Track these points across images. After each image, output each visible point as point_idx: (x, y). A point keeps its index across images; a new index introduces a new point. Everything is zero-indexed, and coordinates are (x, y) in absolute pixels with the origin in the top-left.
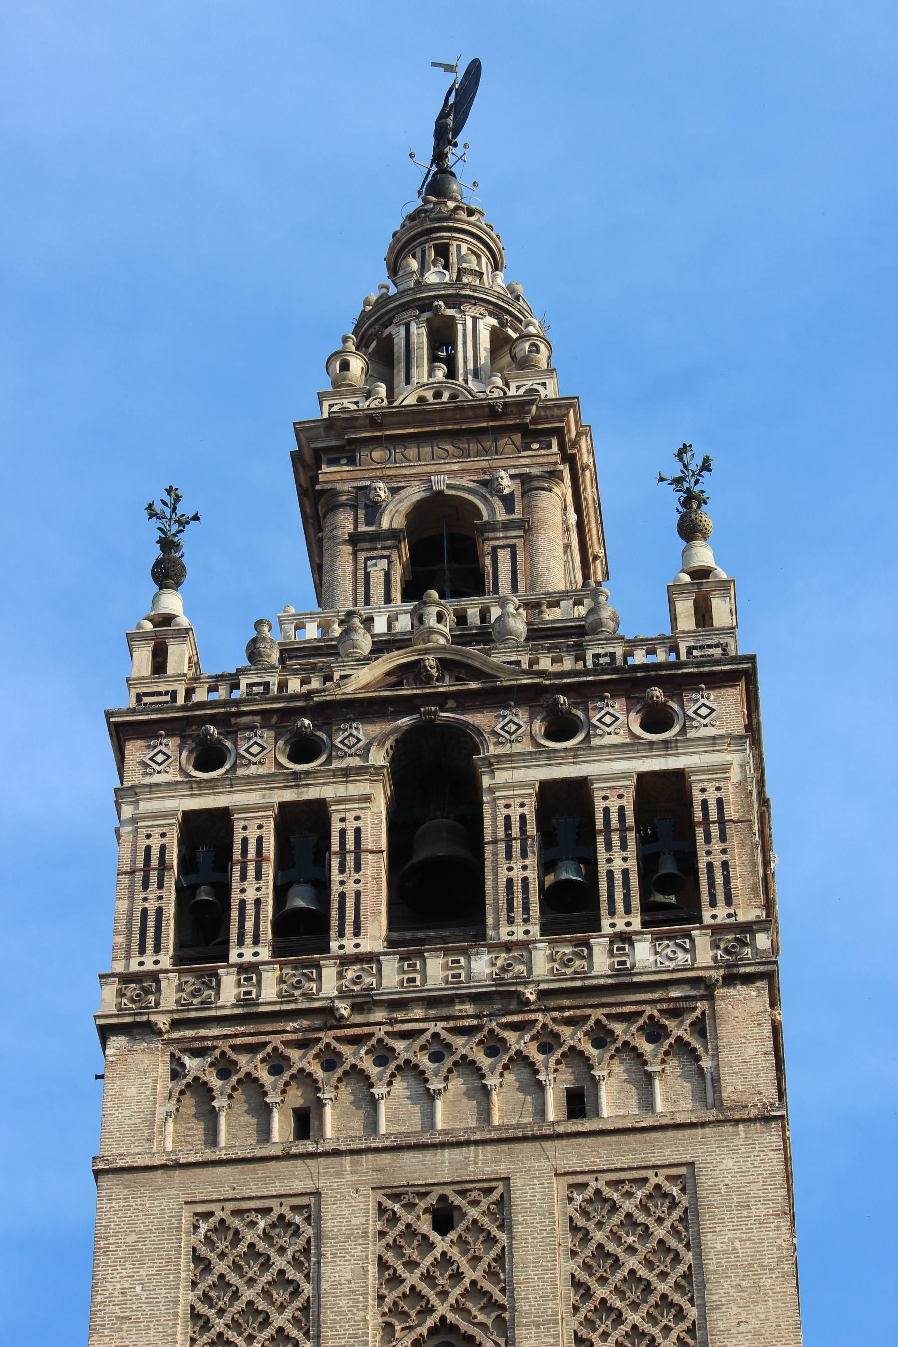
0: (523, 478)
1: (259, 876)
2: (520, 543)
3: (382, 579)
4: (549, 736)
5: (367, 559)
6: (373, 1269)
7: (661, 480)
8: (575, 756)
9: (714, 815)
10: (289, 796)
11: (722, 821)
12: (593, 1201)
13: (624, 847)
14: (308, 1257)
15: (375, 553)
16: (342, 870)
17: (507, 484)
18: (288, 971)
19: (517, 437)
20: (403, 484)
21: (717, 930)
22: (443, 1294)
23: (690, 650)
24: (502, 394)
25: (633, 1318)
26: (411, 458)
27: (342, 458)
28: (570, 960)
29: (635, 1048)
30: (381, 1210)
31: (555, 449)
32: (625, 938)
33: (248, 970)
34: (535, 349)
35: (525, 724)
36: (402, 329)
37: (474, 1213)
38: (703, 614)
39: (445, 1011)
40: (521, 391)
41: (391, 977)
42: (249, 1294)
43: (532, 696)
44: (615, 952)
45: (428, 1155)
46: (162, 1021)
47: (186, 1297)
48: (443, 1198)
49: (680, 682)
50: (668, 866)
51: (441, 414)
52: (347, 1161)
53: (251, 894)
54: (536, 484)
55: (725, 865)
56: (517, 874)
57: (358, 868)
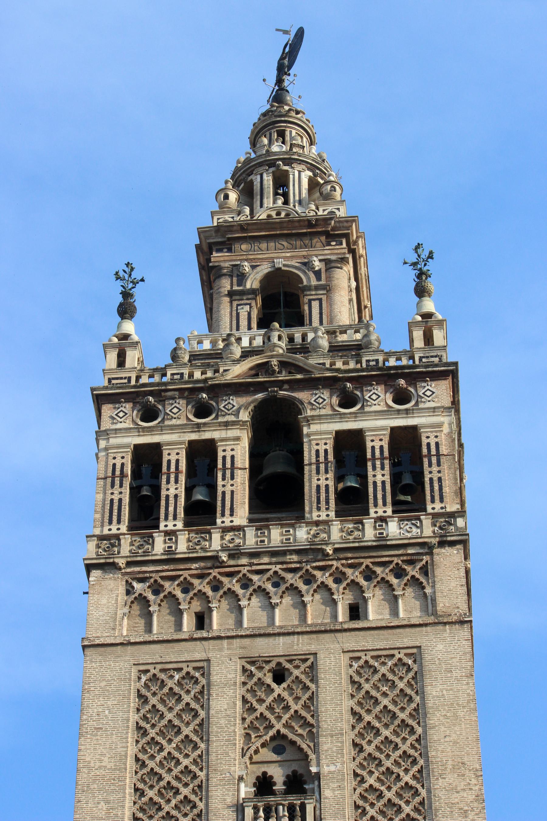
0: (327, 261)
1: (176, 481)
2: (324, 298)
3: (247, 317)
4: (341, 405)
5: (238, 305)
6: (239, 703)
7: (405, 263)
8: (356, 417)
9: (433, 452)
10: (194, 437)
11: (438, 455)
12: (363, 667)
13: (383, 468)
14: (203, 696)
15: (242, 302)
16: (224, 479)
17: (317, 265)
19: (323, 238)
20: (258, 264)
21: (435, 516)
22: (279, 718)
23: (421, 358)
24: (315, 214)
25: (386, 733)
26: (263, 249)
27: (224, 248)
28: (352, 531)
29: (388, 582)
30: (244, 670)
31: (344, 245)
32: (383, 520)
33: (170, 534)
34: (334, 189)
35: (327, 399)
36: (259, 177)
37: (296, 672)
38: (428, 339)
39: (281, 559)
40: (326, 213)
41: (251, 539)
42: (169, 716)
43: (331, 383)
44: (377, 527)
45: (271, 640)
46: (121, 562)
47: (134, 717)
48: (279, 664)
49: (416, 376)
50: (407, 480)
51: (281, 225)
52: (226, 641)
53: (172, 492)
54: (333, 265)
55: (440, 479)
56: (323, 483)
57: (232, 478)
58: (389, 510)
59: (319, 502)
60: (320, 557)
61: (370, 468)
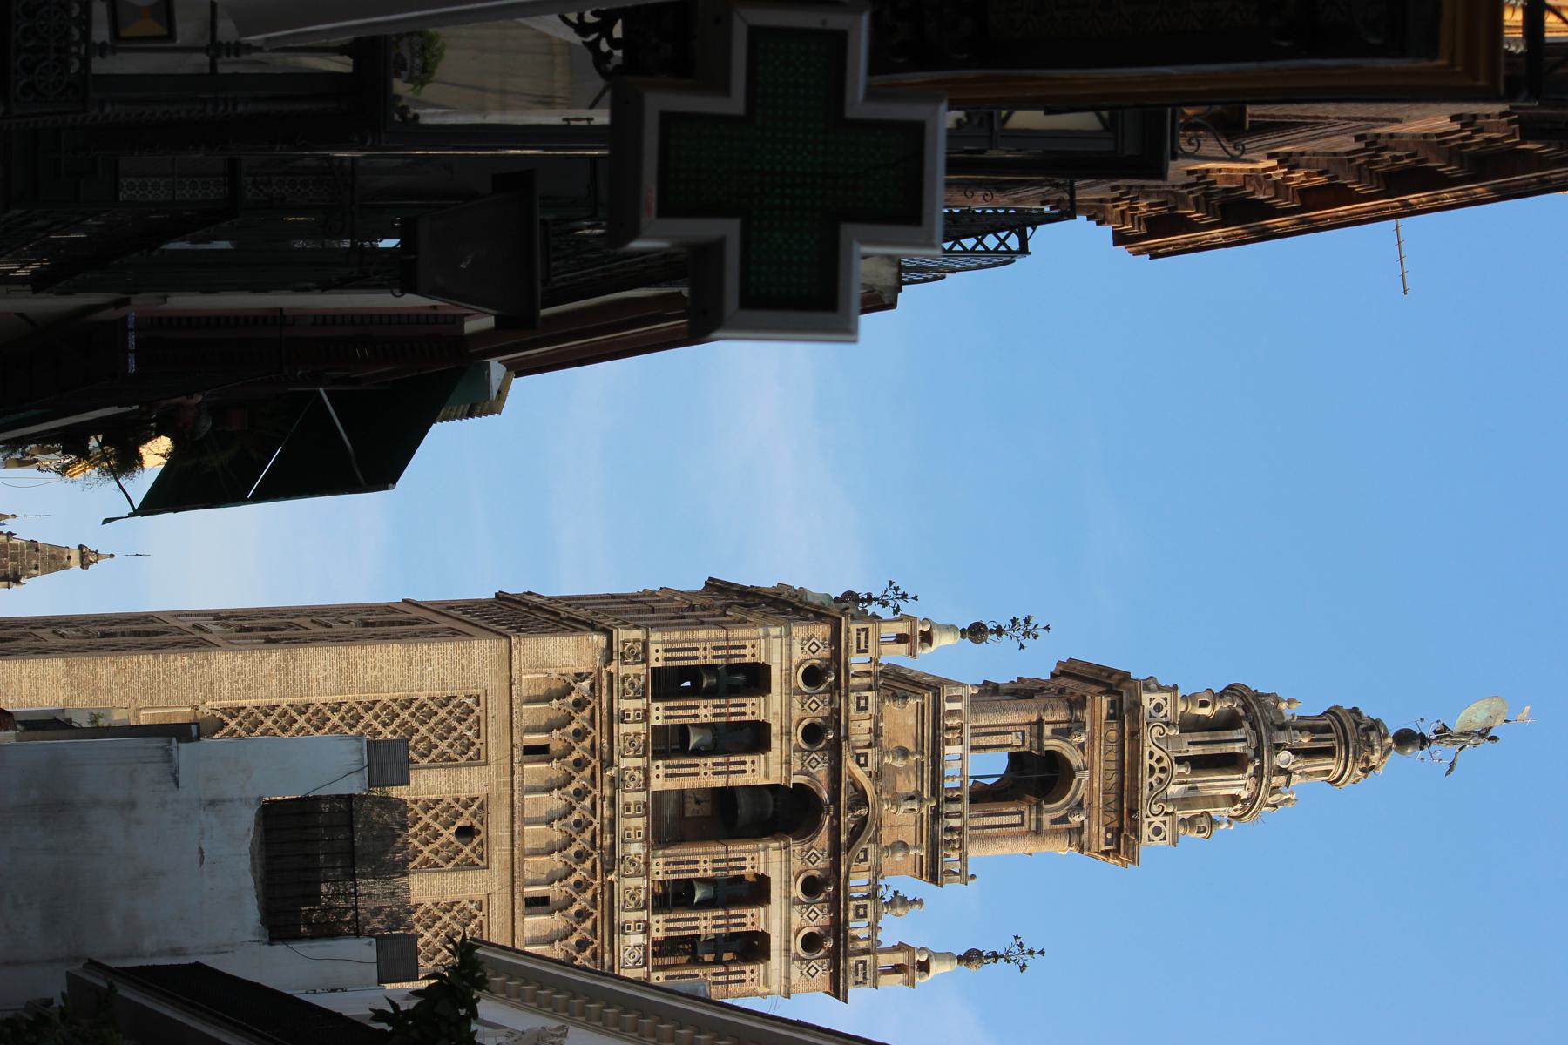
6: (434, 797)
10: (775, 729)
11: (728, 982)
14: (447, 760)
17: (1076, 820)
19: (1116, 825)
23: (864, 962)
30: (474, 799)
32: (647, 929)
33: (645, 715)
39: (607, 829)
42: (423, 730)
45: (508, 824)
46: (612, 668)
48: (479, 832)
53: (702, 712)
54: (1075, 837)
56: (701, 866)
58: (660, 935)
59: (676, 863)
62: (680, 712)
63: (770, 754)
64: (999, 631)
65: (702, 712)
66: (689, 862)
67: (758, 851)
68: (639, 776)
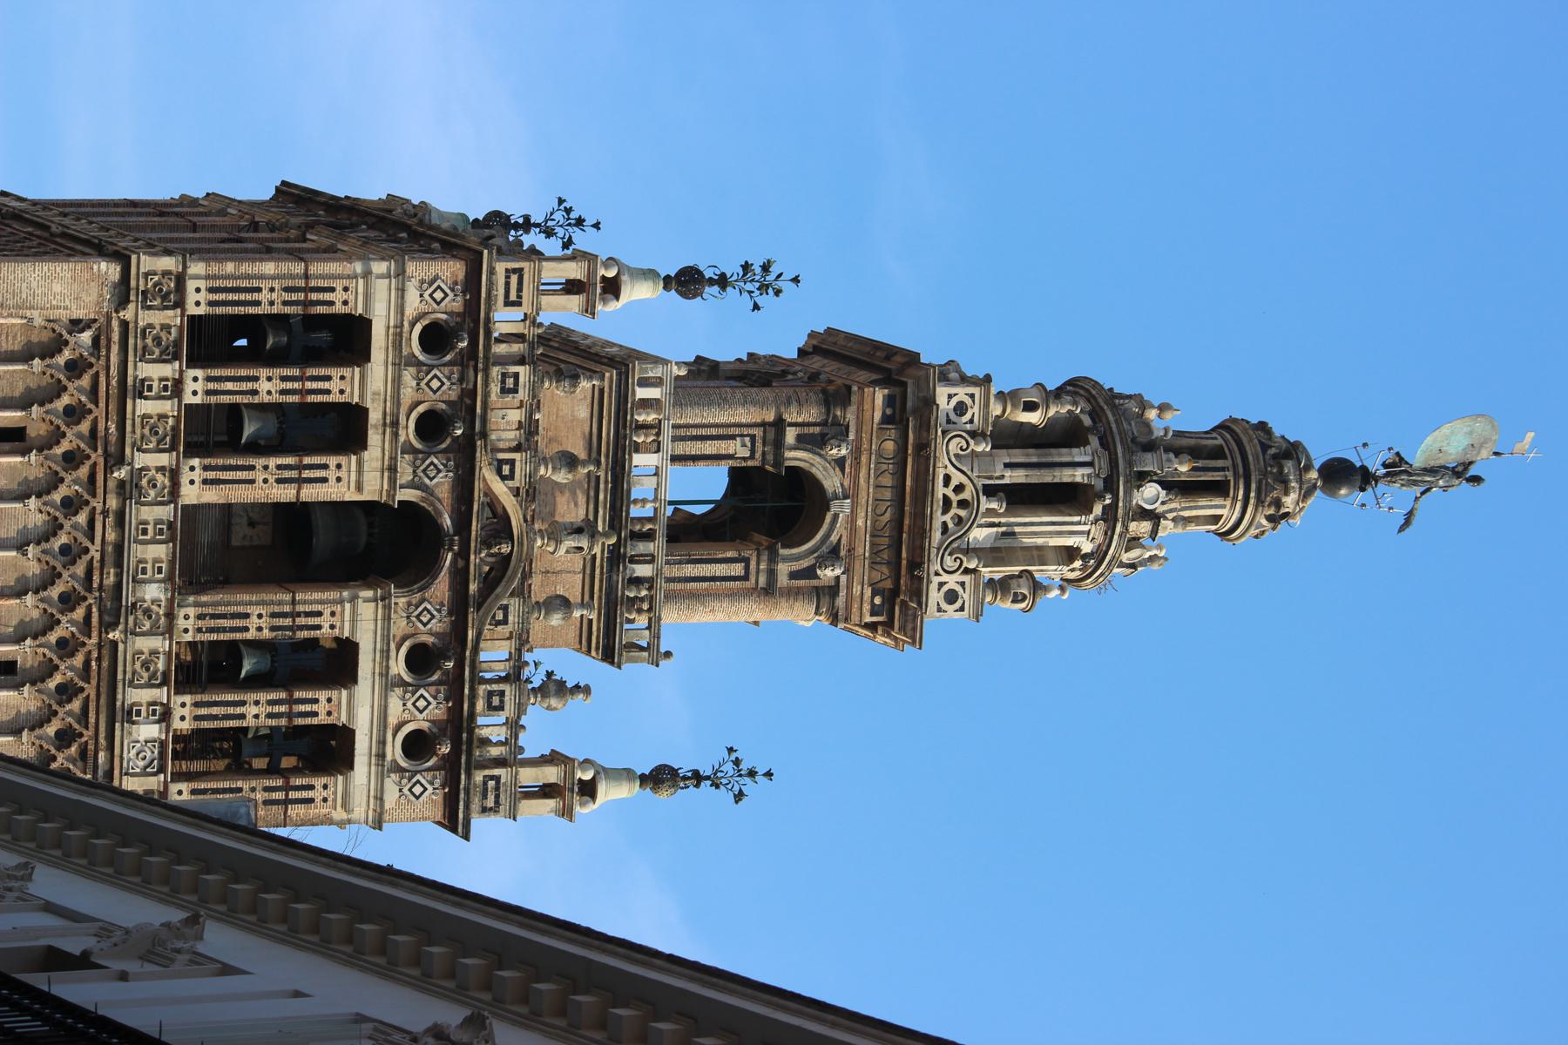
2: (747, 584)
5: (753, 438)
8: (381, 675)
10: (375, 416)
11: (287, 802)
15: (759, 444)
16: (279, 467)
17: (828, 574)
18: (171, 421)
19: (888, 584)
20: (847, 470)
23: (497, 779)
28: (148, 669)
32: (165, 716)
33: (177, 388)
36: (1087, 459)
39: (109, 559)
46: (128, 314)
53: (264, 386)
54: (825, 601)
58: (185, 726)
59: (214, 617)
60: (107, 618)
61: (273, 696)
62: (229, 386)
63: (366, 455)
64: (722, 281)
65: (264, 386)
66: (234, 616)
67: (341, 602)
68: (162, 480)
